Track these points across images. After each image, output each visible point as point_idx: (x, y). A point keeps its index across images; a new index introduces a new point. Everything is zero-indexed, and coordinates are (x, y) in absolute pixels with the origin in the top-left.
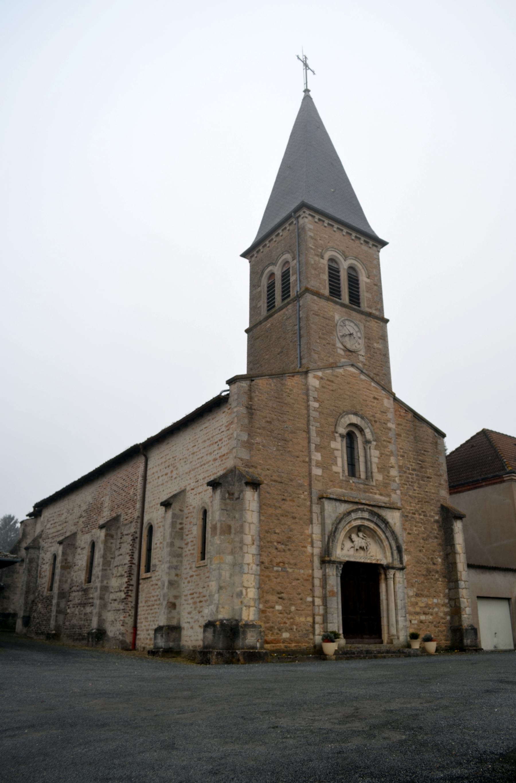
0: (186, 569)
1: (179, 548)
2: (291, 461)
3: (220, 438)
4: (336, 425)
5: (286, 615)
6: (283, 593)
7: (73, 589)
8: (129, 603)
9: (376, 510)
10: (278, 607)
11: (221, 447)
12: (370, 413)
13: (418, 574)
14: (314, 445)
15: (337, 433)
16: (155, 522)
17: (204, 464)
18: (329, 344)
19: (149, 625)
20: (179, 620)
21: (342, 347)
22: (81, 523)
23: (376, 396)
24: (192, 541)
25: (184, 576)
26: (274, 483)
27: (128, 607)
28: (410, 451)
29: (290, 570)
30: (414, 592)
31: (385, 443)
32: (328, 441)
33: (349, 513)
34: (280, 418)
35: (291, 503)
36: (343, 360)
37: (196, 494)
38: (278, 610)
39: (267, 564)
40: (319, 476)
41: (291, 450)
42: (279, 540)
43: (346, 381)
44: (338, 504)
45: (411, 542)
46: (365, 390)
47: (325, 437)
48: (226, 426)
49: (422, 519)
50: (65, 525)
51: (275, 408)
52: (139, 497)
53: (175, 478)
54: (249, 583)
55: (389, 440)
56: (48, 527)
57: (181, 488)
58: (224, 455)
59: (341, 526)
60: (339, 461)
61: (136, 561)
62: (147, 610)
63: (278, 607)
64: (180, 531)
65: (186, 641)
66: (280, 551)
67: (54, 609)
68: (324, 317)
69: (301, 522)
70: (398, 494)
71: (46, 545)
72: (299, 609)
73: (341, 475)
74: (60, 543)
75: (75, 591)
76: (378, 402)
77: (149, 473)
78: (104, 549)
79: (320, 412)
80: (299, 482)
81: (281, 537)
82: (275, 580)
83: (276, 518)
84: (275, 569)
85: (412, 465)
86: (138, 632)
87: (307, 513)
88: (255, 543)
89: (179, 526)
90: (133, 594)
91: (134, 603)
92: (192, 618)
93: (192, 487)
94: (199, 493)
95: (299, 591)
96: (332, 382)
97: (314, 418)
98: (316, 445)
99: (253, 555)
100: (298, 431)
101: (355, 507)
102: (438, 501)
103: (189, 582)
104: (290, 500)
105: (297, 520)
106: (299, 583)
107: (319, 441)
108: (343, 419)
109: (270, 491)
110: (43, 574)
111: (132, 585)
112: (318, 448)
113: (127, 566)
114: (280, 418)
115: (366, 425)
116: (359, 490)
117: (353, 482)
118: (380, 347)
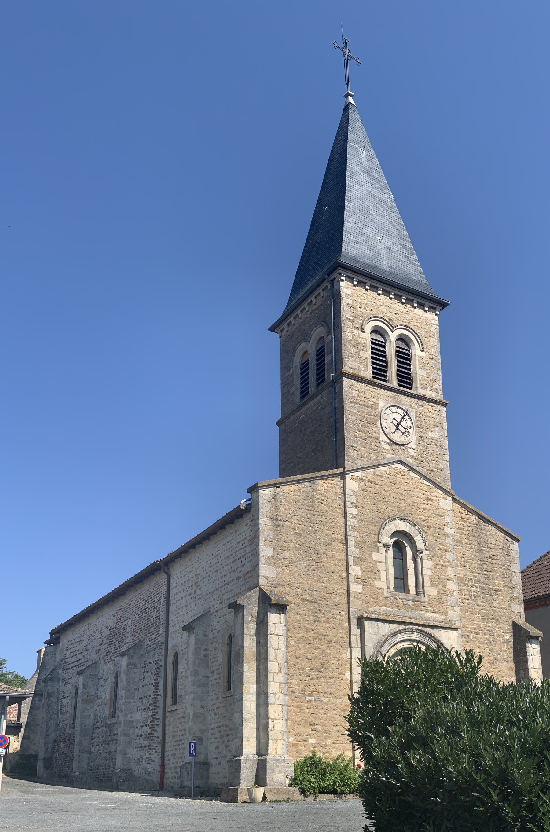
0: (212, 700)
1: (204, 677)
2: (325, 577)
3: (243, 554)
4: (379, 534)
5: (321, 749)
6: (317, 725)
7: (96, 726)
8: (156, 739)
9: (427, 630)
11: (244, 565)
12: (422, 517)
14: (352, 558)
15: (380, 542)
16: (180, 648)
17: (228, 583)
18: (371, 437)
19: (177, 762)
20: (207, 755)
22: (102, 650)
23: (430, 497)
24: (218, 669)
25: (210, 708)
26: (304, 603)
27: (155, 743)
28: (473, 559)
29: (325, 700)
31: (440, 551)
32: (370, 552)
33: (395, 634)
34: (310, 528)
35: (325, 625)
36: (388, 456)
37: (220, 617)
38: (311, 744)
39: (297, 694)
40: (358, 593)
41: (324, 564)
42: (312, 666)
44: (380, 624)
46: (415, 490)
47: (366, 547)
48: (250, 540)
50: (86, 653)
51: (305, 518)
52: (162, 621)
53: (199, 599)
55: (445, 548)
56: (67, 656)
57: (205, 610)
58: (248, 573)
60: (383, 574)
61: (161, 692)
62: (174, 746)
64: (204, 658)
65: (214, 778)
66: (312, 679)
67: (76, 747)
70: (456, 610)
71: (66, 677)
72: (336, 742)
73: (385, 590)
74: (80, 673)
75: (99, 728)
76: (432, 503)
77: (172, 593)
78: (127, 679)
79: (359, 520)
80: (335, 600)
81: (314, 663)
82: (307, 710)
83: (308, 642)
84: (308, 698)
85: (475, 576)
86: (166, 771)
87: (344, 636)
88: (282, 669)
89: (203, 653)
90: (160, 729)
91: (160, 738)
92: (219, 753)
93: (217, 609)
94: (224, 616)
96: (374, 483)
97: (352, 526)
98: (354, 557)
99: (280, 684)
100: (333, 543)
101: (402, 627)
102: (509, 617)
103: (215, 714)
104: (324, 622)
105: (333, 644)
106: (335, 714)
107: (358, 553)
108: (387, 526)
109: (301, 612)
110: (64, 709)
111: (158, 719)
112: (358, 561)
113: (151, 698)
114: (310, 528)
115: (417, 532)
118: (436, 437)
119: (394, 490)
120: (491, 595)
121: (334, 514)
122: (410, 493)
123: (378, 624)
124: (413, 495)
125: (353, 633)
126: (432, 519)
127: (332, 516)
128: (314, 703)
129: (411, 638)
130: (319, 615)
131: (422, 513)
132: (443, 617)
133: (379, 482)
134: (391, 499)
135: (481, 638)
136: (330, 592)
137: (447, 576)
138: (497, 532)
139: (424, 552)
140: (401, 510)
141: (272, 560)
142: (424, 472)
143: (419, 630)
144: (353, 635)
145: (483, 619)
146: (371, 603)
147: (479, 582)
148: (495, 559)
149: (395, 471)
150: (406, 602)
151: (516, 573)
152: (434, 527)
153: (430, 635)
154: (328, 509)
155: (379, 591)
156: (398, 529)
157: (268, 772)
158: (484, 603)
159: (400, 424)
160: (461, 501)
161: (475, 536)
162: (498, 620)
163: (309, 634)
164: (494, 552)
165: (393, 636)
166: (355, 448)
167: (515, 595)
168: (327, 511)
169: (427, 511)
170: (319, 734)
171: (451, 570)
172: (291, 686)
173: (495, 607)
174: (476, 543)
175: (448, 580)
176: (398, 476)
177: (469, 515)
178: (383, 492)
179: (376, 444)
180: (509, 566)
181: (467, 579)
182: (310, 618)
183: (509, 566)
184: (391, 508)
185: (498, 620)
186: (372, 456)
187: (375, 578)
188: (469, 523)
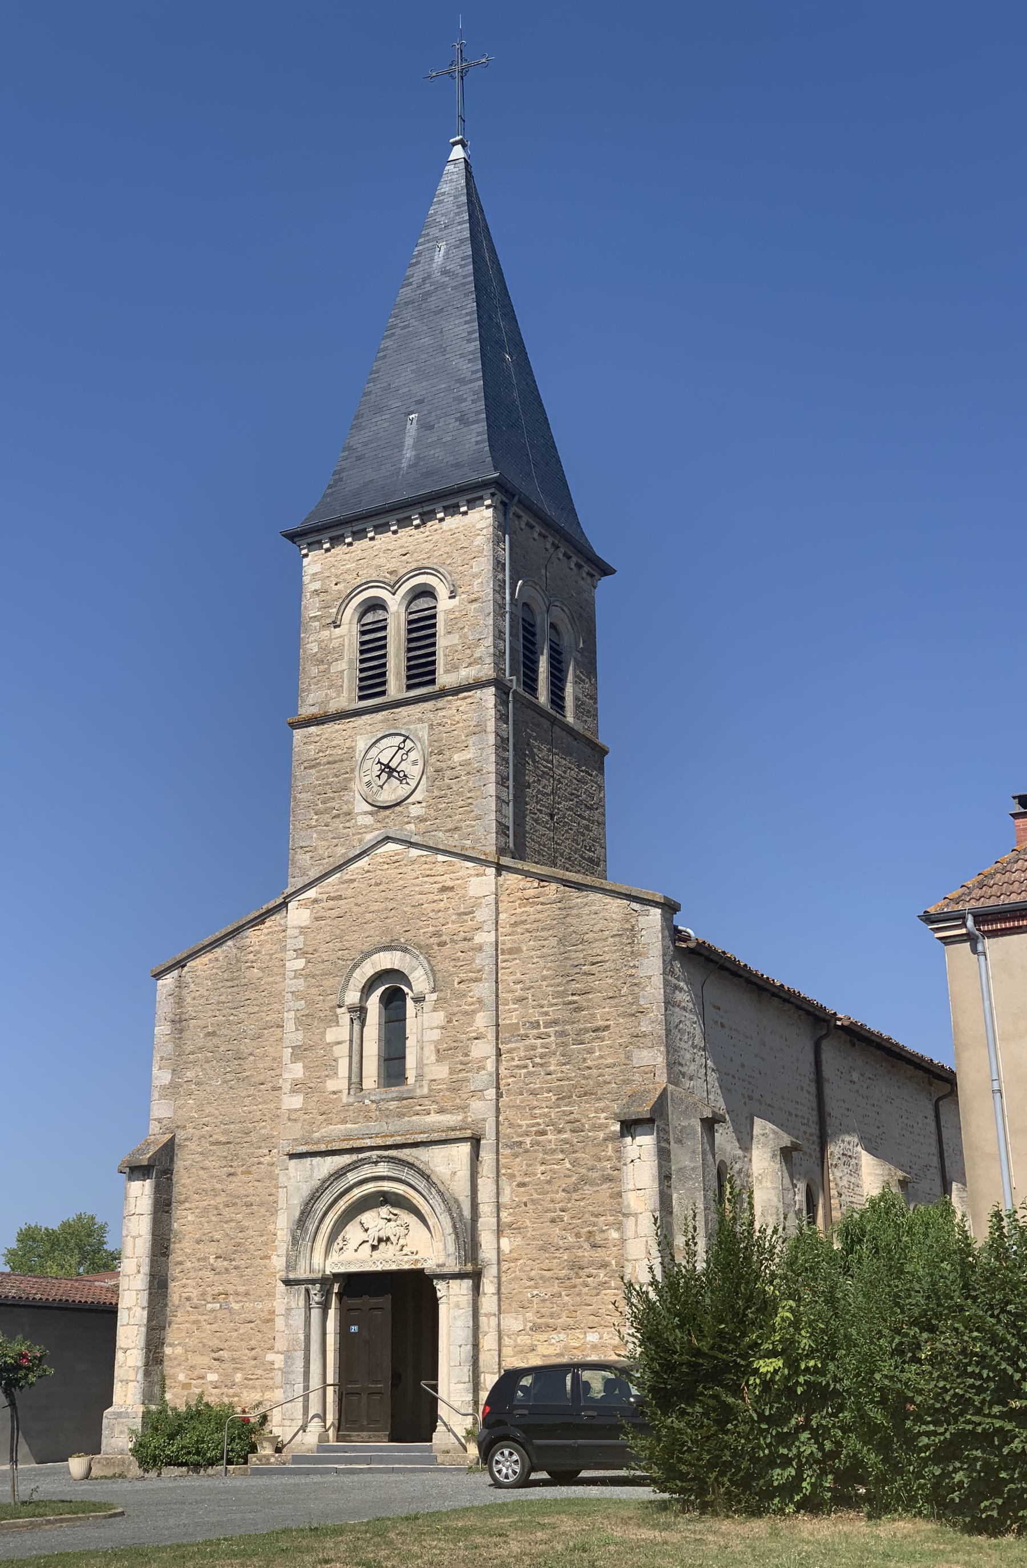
6: (222, 1350)
10: (212, 1377)
13: (542, 1278)
14: (290, 1050)
15: (340, 1007)
21: (370, 808)
28: (544, 978)
29: (236, 1306)
30: (525, 1320)
32: (322, 1030)
33: (339, 1174)
38: (211, 1382)
39: (195, 1301)
40: (296, 1110)
42: (220, 1252)
43: (373, 881)
45: (526, 1205)
49: (566, 1142)
51: (223, 1003)
54: (130, 1341)
59: (321, 1205)
63: (212, 1377)
66: (219, 1273)
68: (329, 763)
69: (263, 1210)
72: (249, 1376)
76: (451, 894)
79: (306, 977)
80: (263, 1131)
83: (215, 1212)
84: (209, 1306)
85: (546, 1014)
95: (253, 1343)
96: (340, 898)
97: (292, 992)
100: (266, 1032)
101: (355, 1157)
104: (243, 1173)
106: (251, 1329)
107: (300, 1038)
108: (358, 970)
114: (231, 1018)
115: (415, 963)
116: (387, 1114)
117: (372, 1101)
118: (468, 757)
119: (376, 896)
120: (583, 1044)
121: (271, 979)
122: (406, 891)
123: (311, 1161)
124: (413, 893)
125: (282, 1185)
126: (450, 925)
127: (268, 984)
128: (219, 1314)
129: (373, 1174)
130: (235, 1164)
131: (429, 922)
132: (460, 1118)
133: (349, 893)
134: (369, 916)
135: (550, 1141)
136: (255, 1120)
137: (474, 1031)
138: (608, 900)
139: (427, 999)
140: (387, 931)
141: (169, 1090)
142: (441, 839)
143: (385, 1157)
144: (281, 1187)
145: (558, 1099)
146: (318, 1123)
147: (555, 1022)
148: (598, 962)
149: (381, 860)
150: (384, 1105)
151: (650, 977)
152: (452, 941)
153: (408, 1163)
154: (261, 974)
155: (335, 1096)
156: (378, 969)
157: (105, 1432)
158: (564, 1064)
159: (387, 766)
160: (519, 866)
161: (552, 928)
162: (595, 1094)
163: (219, 1199)
164: (597, 948)
165: (336, 1179)
166: (307, 849)
167: (645, 1028)
168: (259, 979)
169: (440, 914)
170: (224, 1366)
171: (484, 1017)
172: (186, 1290)
173: (590, 1068)
174: (554, 941)
175: (476, 1039)
176: (386, 866)
177: (543, 887)
178: (356, 909)
179: (347, 824)
180: (634, 967)
181: (528, 1024)
182: (221, 1172)
183: (634, 967)
184: (367, 934)
185: (595, 1094)
186: (339, 848)
187: (327, 1076)
188: (542, 904)
